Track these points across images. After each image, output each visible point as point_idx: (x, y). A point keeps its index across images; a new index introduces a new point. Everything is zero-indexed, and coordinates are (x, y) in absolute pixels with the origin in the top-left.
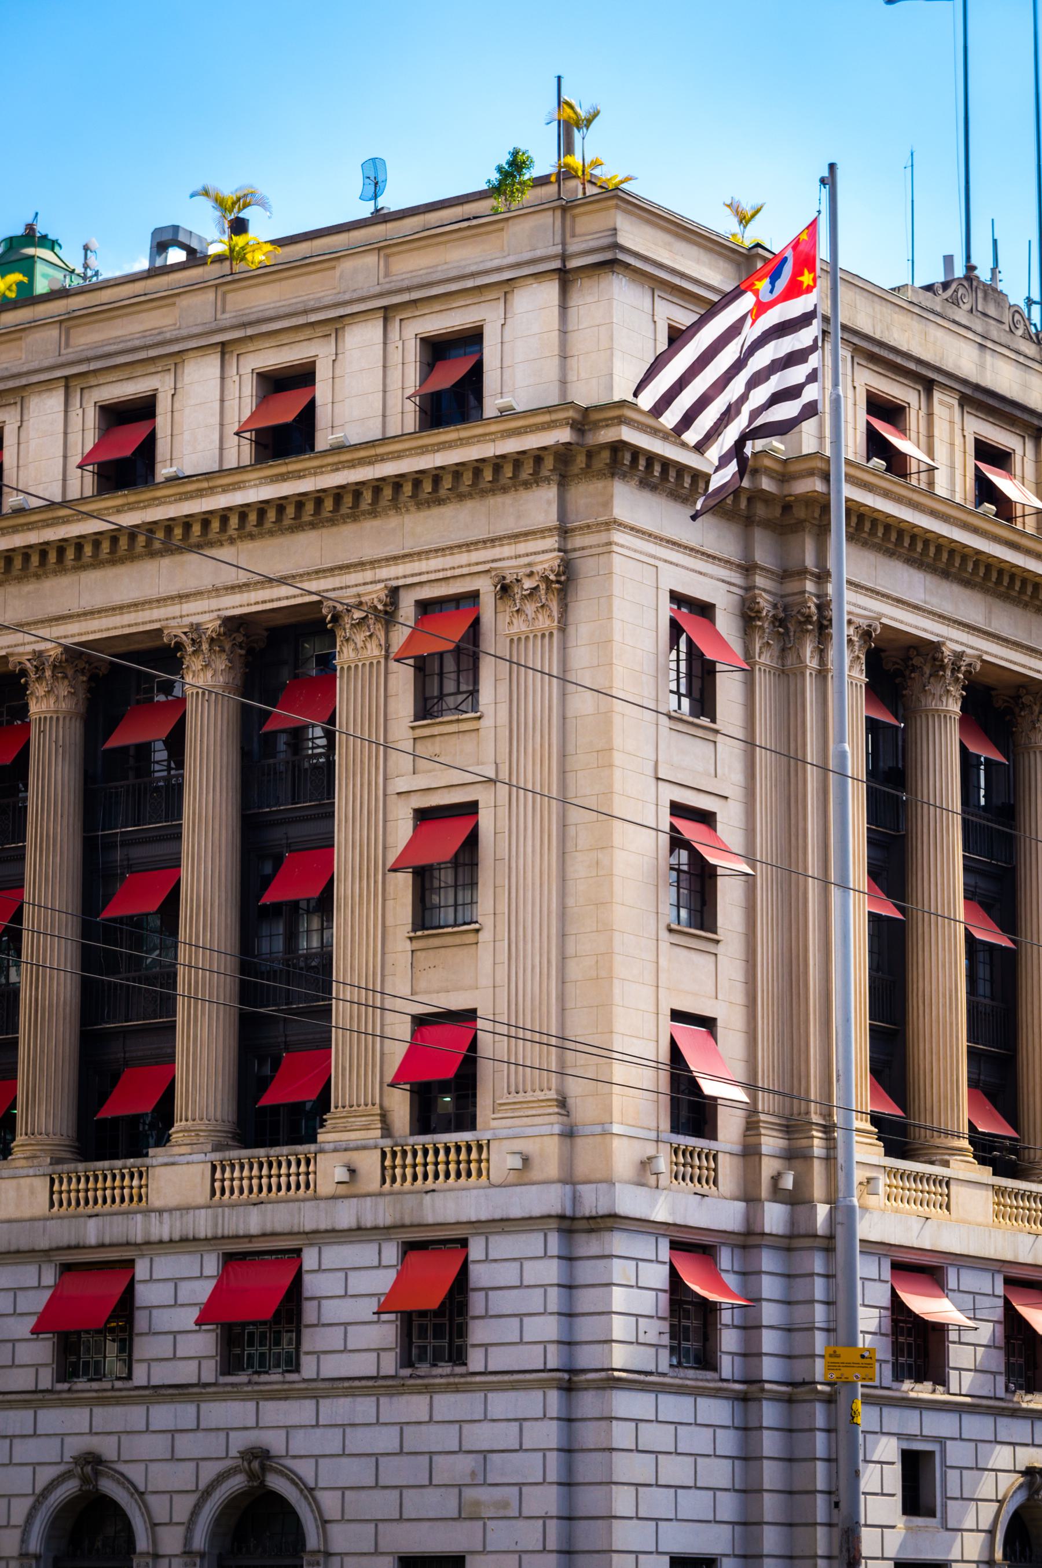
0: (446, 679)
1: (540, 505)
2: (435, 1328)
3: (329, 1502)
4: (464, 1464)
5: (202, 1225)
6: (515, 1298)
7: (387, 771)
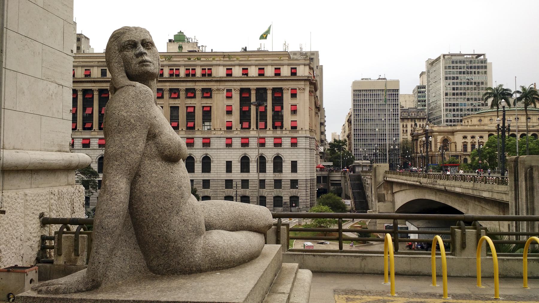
0: (294, 95)
1: (303, 83)
2: (294, 145)
3: (285, 157)
4: (297, 154)
5: (272, 136)
6: (302, 143)
7: (287, 101)
